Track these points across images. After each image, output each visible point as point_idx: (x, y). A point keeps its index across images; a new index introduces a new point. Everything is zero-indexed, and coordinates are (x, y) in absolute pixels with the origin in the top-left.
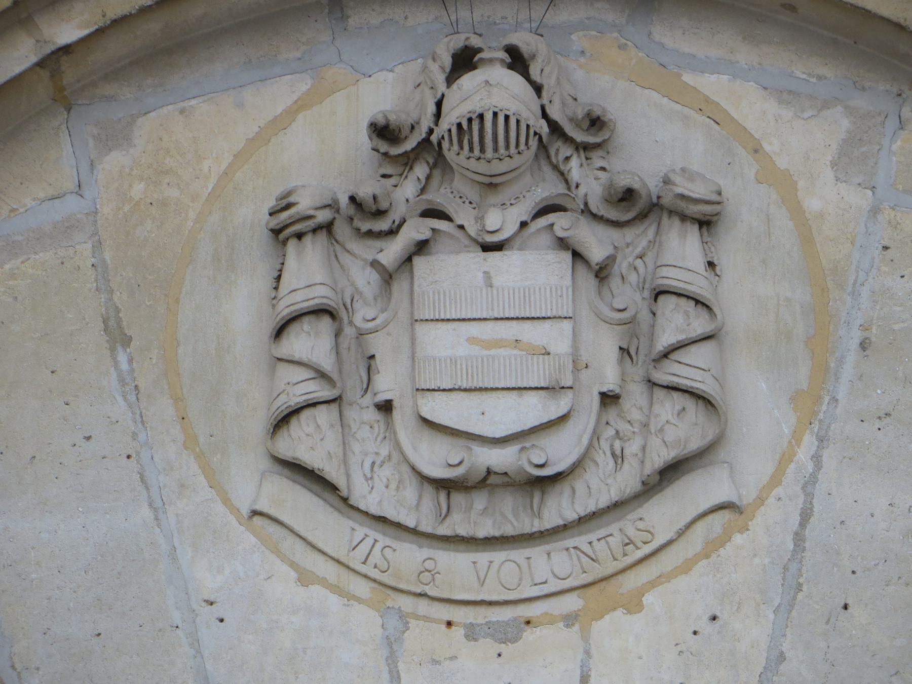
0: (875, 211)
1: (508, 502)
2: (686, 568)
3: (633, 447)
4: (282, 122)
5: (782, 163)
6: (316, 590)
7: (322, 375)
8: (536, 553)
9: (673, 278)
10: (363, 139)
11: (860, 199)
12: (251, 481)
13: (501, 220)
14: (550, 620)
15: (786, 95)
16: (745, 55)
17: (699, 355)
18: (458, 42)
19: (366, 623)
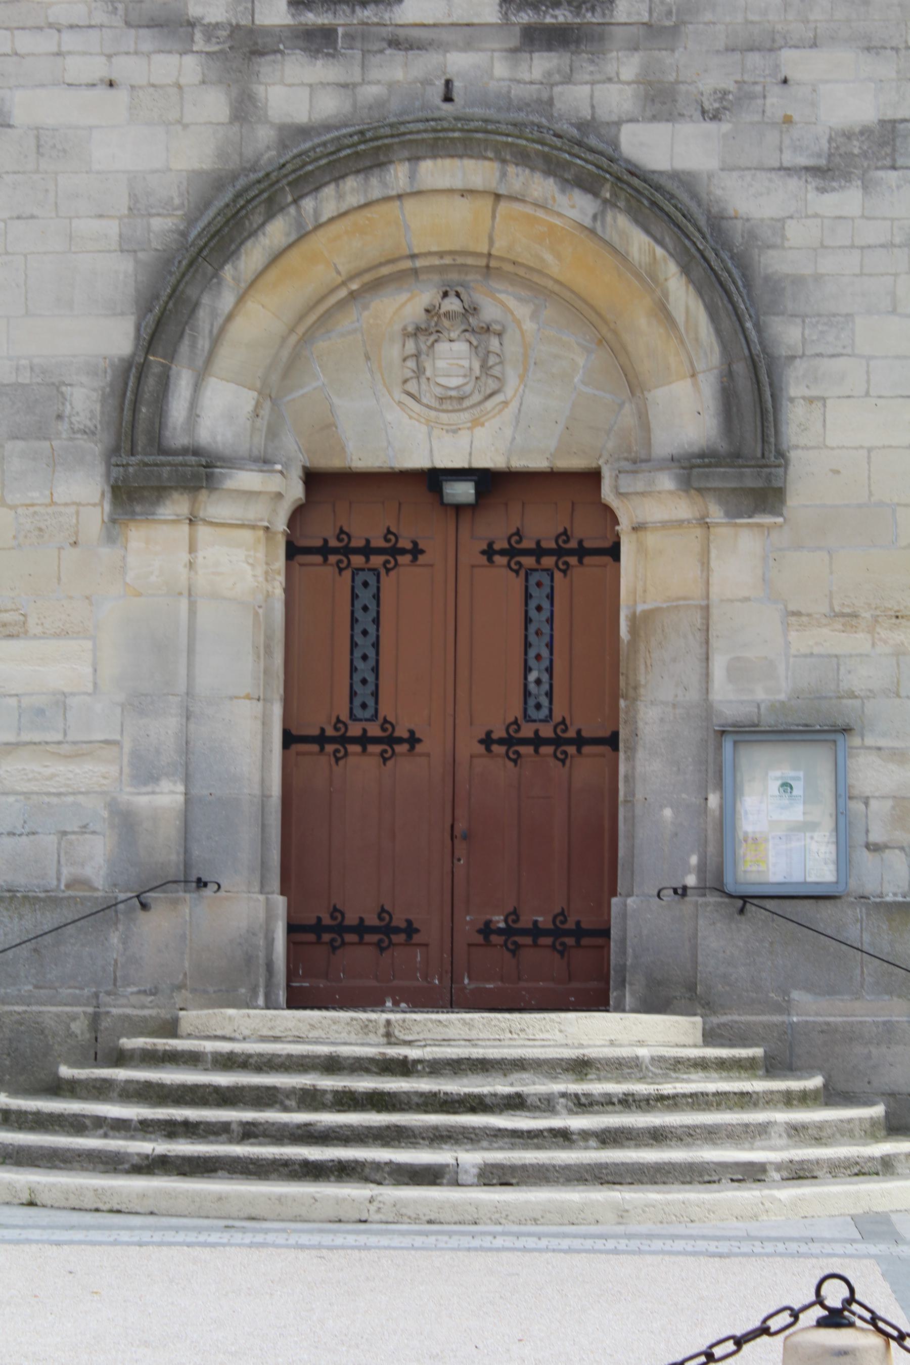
0: (539, 330)
1: (455, 402)
2: (494, 416)
3: (483, 389)
4: (403, 305)
5: (518, 317)
6: (413, 421)
7: (414, 371)
8: (462, 414)
9: (492, 349)
10: (423, 312)
11: (535, 326)
12: (399, 396)
13: (453, 335)
14: (464, 428)
15: (520, 299)
16: (510, 289)
17: (498, 368)
18: (444, 289)
19: (424, 429)
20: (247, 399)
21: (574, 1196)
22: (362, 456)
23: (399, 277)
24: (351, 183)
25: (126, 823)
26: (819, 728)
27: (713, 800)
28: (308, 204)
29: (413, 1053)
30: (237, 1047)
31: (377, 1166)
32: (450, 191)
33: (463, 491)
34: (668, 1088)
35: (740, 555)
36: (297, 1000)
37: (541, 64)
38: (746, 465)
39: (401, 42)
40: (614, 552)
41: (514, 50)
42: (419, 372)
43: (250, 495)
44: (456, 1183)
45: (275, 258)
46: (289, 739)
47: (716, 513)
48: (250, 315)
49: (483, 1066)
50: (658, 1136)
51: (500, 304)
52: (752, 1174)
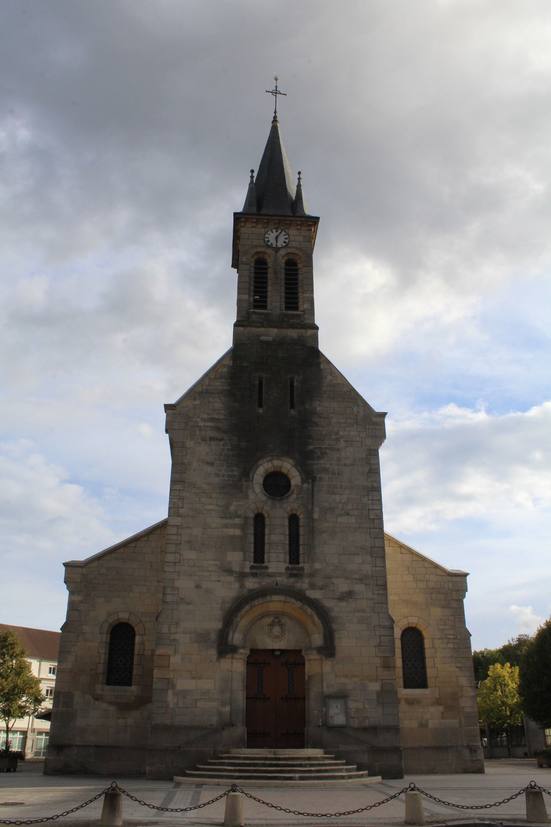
20: (241, 636)
21: (316, 782)
22: (261, 646)
23: (266, 615)
24: (260, 599)
25: (220, 714)
26: (342, 696)
27: (324, 709)
28: (253, 602)
29: (281, 756)
30: (248, 756)
31: (281, 777)
32: (277, 601)
33: (278, 653)
34: (325, 762)
35: (328, 666)
36: (249, 747)
37: (292, 580)
38: (328, 649)
39: (269, 575)
40: (304, 664)
41: (288, 577)
42: (271, 632)
43: (242, 654)
44: (295, 780)
45: (247, 612)
46: (247, 698)
47: (323, 657)
48: (242, 622)
49: (293, 759)
50: (326, 771)
51: (285, 620)
52: (342, 777)
